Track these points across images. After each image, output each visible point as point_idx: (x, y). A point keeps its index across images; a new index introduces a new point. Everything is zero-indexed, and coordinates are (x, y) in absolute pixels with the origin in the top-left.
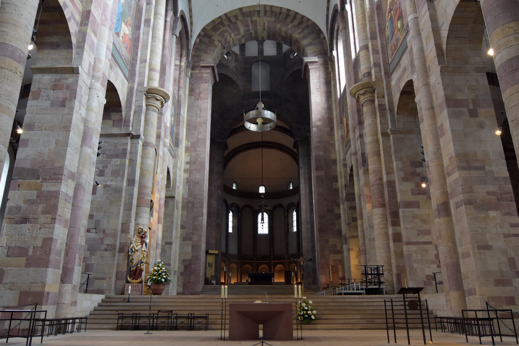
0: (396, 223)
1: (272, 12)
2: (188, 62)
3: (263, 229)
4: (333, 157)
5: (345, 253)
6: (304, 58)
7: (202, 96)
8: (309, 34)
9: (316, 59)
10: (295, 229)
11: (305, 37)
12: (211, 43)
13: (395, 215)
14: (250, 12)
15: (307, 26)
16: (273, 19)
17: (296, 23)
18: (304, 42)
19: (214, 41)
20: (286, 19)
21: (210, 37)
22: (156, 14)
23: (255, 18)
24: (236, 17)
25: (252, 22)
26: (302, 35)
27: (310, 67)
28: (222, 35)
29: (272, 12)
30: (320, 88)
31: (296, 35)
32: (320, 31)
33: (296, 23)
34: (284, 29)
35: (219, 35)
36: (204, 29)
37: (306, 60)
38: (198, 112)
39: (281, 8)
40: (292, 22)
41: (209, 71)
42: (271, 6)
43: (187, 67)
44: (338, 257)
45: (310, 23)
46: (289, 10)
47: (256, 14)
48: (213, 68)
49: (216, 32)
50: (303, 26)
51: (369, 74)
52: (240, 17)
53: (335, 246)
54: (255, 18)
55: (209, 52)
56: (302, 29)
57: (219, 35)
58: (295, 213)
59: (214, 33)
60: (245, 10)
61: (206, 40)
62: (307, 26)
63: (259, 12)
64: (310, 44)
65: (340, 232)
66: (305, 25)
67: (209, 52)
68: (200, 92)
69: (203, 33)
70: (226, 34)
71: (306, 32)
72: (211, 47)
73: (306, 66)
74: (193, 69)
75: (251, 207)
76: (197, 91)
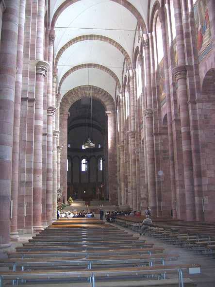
0: (127, 187)
1: (93, 88)
3: (84, 168)
4: (115, 154)
5: (119, 190)
7: (64, 127)
8: (108, 99)
9: (110, 112)
10: (101, 169)
11: (106, 101)
12: (67, 102)
13: (127, 185)
16: (93, 92)
17: (103, 94)
18: (106, 103)
20: (98, 92)
21: (67, 99)
24: (77, 90)
26: (105, 100)
27: (108, 115)
28: (71, 98)
31: (103, 100)
34: (98, 97)
35: (71, 98)
37: (107, 112)
41: (67, 115)
44: (115, 191)
46: (100, 88)
48: (68, 114)
50: (106, 95)
51: (123, 141)
53: (115, 187)
57: (71, 98)
58: (101, 161)
61: (65, 101)
64: (108, 105)
65: (117, 182)
66: (106, 95)
68: (63, 125)
70: (74, 99)
71: (107, 98)
75: (79, 158)
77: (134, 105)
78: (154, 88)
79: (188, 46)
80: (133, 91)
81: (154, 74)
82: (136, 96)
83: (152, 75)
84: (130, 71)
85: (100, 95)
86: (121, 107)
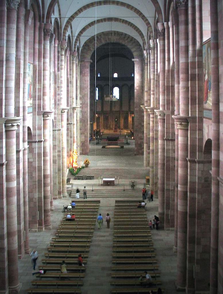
1: (118, 34)
2: (79, 60)
6: (132, 59)
7: (86, 74)
12: (89, 49)
14: (107, 33)
15: (134, 42)
17: (129, 40)
18: (133, 50)
19: (90, 48)
20: (124, 37)
21: (88, 46)
22: (73, 77)
23: (110, 37)
25: (108, 39)
29: (118, 34)
30: (139, 72)
31: (129, 46)
32: (140, 45)
33: (129, 40)
36: (85, 43)
37: (133, 60)
38: (85, 82)
39: (122, 33)
40: (127, 39)
42: (118, 32)
43: (78, 62)
45: (136, 41)
46: (126, 34)
47: (110, 35)
49: (91, 43)
52: (102, 36)
54: (110, 37)
55: (88, 53)
56: (132, 43)
59: (90, 44)
60: (104, 33)
61: (87, 48)
62: (134, 42)
63: (111, 33)
64: (135, 51)
67: (88, 53)
68: (85, 73)
69: (85, 45)
72: (89, 51)
73: (133, 62)
74: (81, 62)
76: (83, 72)
77: (154, 79)
78: (168, 87)
79: (193, 91)
80: (154, 63)
81: (169, 71)
82: (157, 69)
83: (166, 72)
84: (151, 41)
85: (126, 42)
86: (146, 64)
